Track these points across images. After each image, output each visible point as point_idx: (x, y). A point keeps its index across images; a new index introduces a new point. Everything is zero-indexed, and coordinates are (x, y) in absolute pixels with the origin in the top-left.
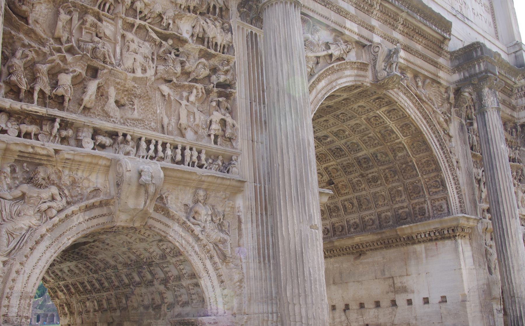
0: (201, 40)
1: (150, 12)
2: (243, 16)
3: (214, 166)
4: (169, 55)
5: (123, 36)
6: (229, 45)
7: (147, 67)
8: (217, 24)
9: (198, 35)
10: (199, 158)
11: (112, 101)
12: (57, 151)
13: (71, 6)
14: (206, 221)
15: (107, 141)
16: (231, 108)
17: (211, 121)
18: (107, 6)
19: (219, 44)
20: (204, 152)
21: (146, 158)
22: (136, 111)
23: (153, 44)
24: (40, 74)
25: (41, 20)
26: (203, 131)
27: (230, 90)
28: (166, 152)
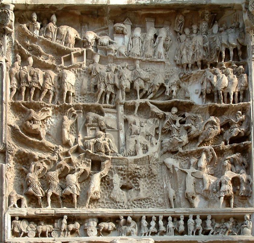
5: (126, 121)
7: (149, 145)
8: (230, 70)
10: (204, 224)
16: (248, 163)
18: (108, 96)
21: (148, 235)
22: (141, 191)
23: (156, 119)
24: (50, 180)
27: (243, 143)
28: (168, 226)
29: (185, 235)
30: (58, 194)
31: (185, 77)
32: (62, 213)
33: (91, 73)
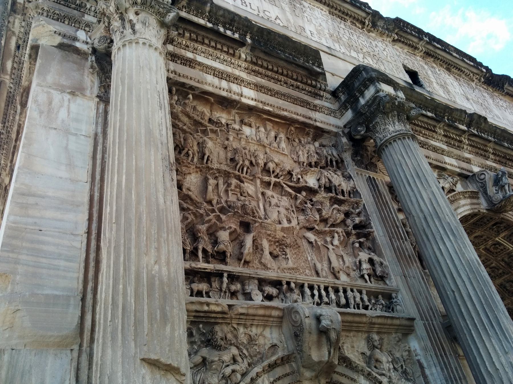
0: (328, 189)
1: (282, 171)
2: (359, 163)
3: (379, 307)
4: (306, 205)
5: (263, 194)
6: (353, 191)
9: (325, 186)
10: (362, 299)
11: (267, 252)
12: (230, 306)
13: (216, 172)
14: (389, 370)
15: (273, 291)
17: (360, 262)
18: (245, 169)
19: (345, 190)
20: (364, 292)
22: (290, 260)
25: (192, 188)
26: (354, 272)
27: (367, 230)
29: (348, 309)
30: (209, 250)
31: (304, 171)
32: (222, 271)
33: (226, 148)
